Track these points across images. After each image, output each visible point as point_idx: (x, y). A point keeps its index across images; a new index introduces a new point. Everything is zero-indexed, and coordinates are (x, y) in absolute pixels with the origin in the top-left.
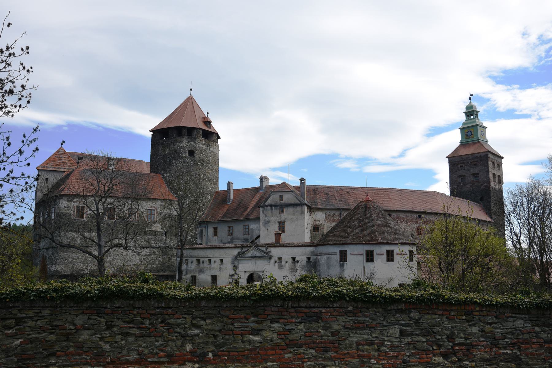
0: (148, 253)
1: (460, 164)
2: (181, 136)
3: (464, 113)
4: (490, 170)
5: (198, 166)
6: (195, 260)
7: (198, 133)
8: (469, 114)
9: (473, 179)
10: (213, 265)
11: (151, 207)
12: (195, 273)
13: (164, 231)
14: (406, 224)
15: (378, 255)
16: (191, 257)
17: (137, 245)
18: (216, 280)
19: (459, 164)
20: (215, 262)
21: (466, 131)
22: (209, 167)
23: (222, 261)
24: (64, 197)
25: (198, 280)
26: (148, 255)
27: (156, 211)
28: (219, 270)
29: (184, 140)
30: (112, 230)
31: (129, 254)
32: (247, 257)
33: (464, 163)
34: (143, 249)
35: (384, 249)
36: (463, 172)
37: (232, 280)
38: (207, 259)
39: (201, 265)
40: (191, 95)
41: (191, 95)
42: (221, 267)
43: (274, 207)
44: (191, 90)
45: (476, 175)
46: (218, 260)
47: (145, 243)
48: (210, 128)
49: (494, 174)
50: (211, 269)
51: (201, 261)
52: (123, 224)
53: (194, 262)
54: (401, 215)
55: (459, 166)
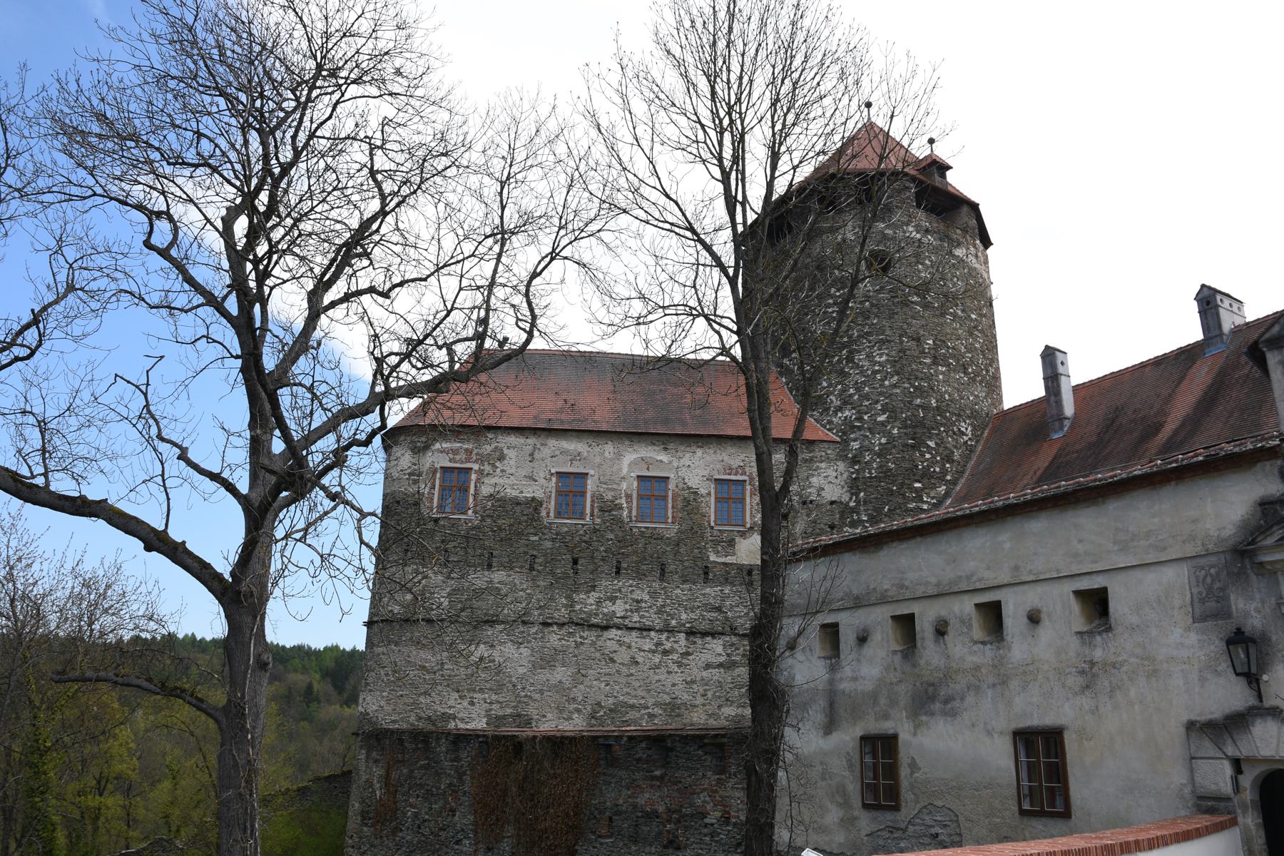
0: (722, 659)
5: (907, 305)
6: (879, 618)
10: (1019, 644)
11: (730, 470)
12: (886, 717)
16: (858, 603)
17: (674, 622)
18: (1058, 773)
20: (1034, 618)
22: (955, 315)
24: (402, 438)
25: (914, 766)
26: (721, 665)
27: (748, 487)
28: (1074, 681)
30: (575, 562)
31: (640, 660)
34: (699, 641)
37: (1228, 770)
38: (966, 606)
39: (930, 653)
42: (1098, 654)
47: (709, 615)
50: (1004, 682)
51: (924, 626)
52: (616, 536)
53: (877, 638)
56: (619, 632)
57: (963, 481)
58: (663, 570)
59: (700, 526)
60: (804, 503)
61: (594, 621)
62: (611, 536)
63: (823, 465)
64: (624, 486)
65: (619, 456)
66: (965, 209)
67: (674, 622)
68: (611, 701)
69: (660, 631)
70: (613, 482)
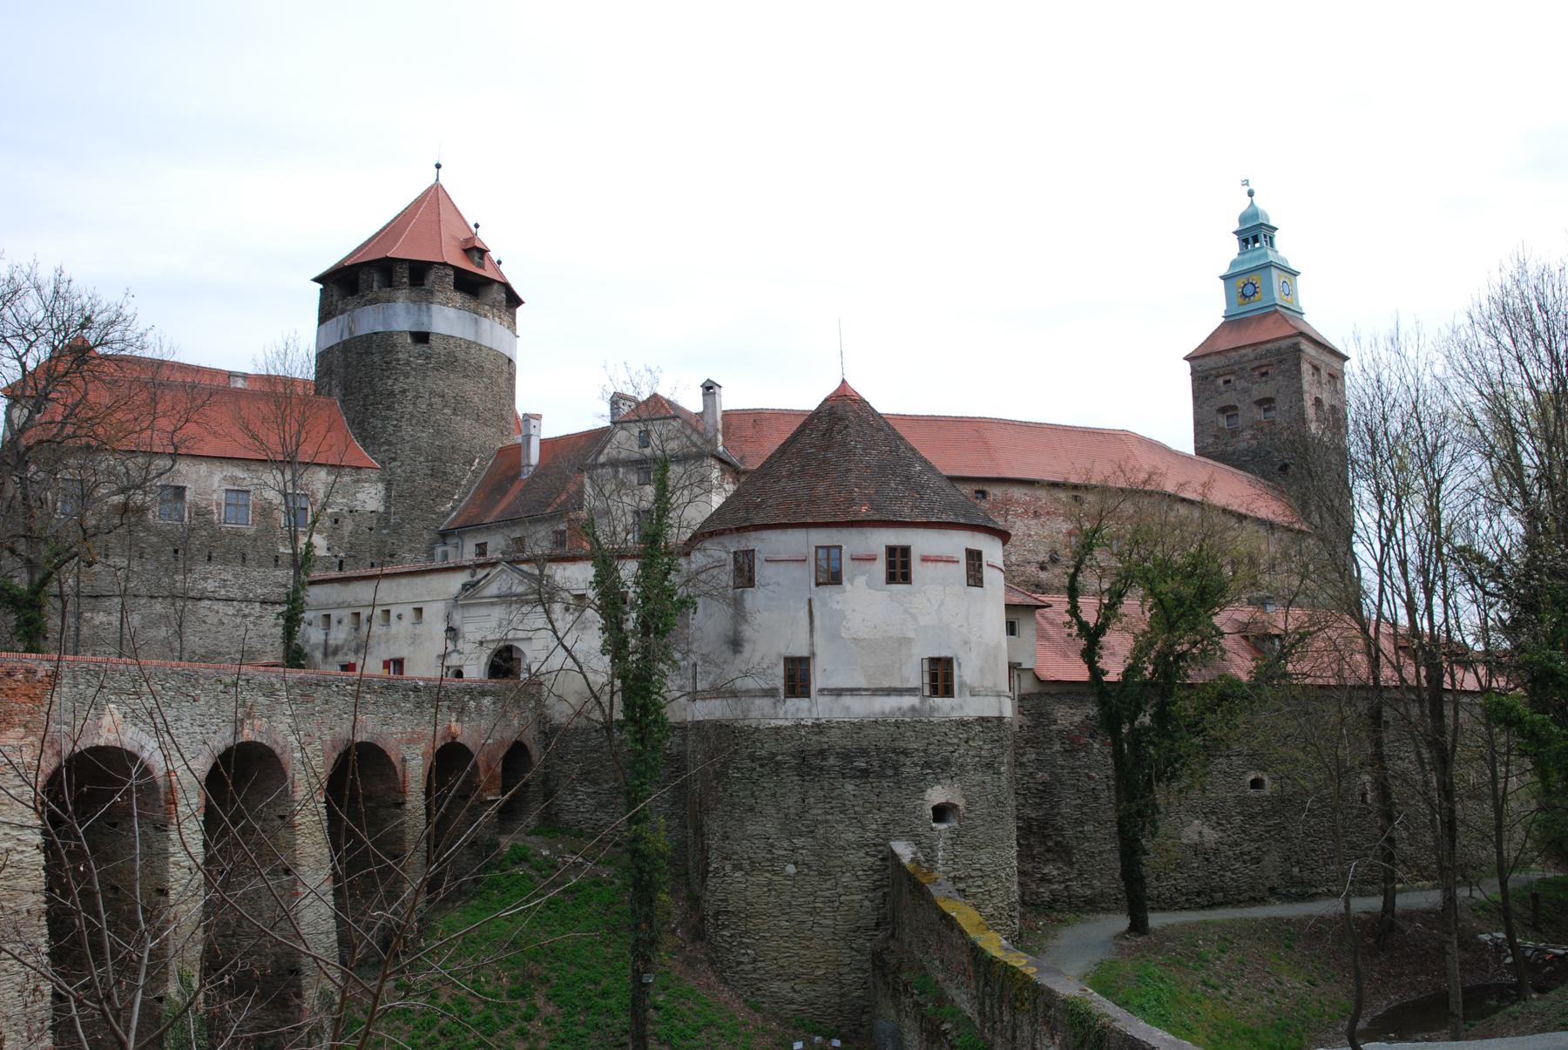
1: (1225, 374)
2: (390, 286)
3: (1235, 233)
4: (1306, 387)
7: (441, 278)
8: (1249, 235)
9: (1259, 415)
12: (346, 654)
13: (336, 556)
14: (1033, 522)
15: (857, 563)
16: (339, 606)
17: (251, 595)
19: (1218, 376)
21: (1240, 282)
23: (419, 611)
29: (398, 298)
30: (176, 551)
31: (226, 621)
32: (490, 597)
33: (1233, 373)
34: (270, 608)
35: (880, 540)
36: (1228, 399)
40: (437, 180)
41: (437, 180)
42: (417, 632)
43: (623, 466)
44: (438, 166)
45: (1266, 403)
46: (408, 612)
48: (482, 266)
49: (1318, 402)
50: (388, 641)
53: (345, 621)
54: (1018, 493)
55: (1220, 381)
56: (210, 602)
57: (467, 499)
58: (244, 558)
59: (273, 527)
60: (351, 512)
61: (191, 594)
62: (204, 533)
63: (367, 485)
64: (215, 496)
65: (211, 474)
66: (496, 286)
67: (251, 595)
68: (203, 650)
69: (241, 601)
70: (206, 493)
